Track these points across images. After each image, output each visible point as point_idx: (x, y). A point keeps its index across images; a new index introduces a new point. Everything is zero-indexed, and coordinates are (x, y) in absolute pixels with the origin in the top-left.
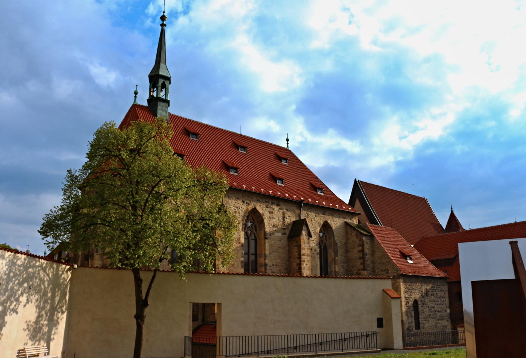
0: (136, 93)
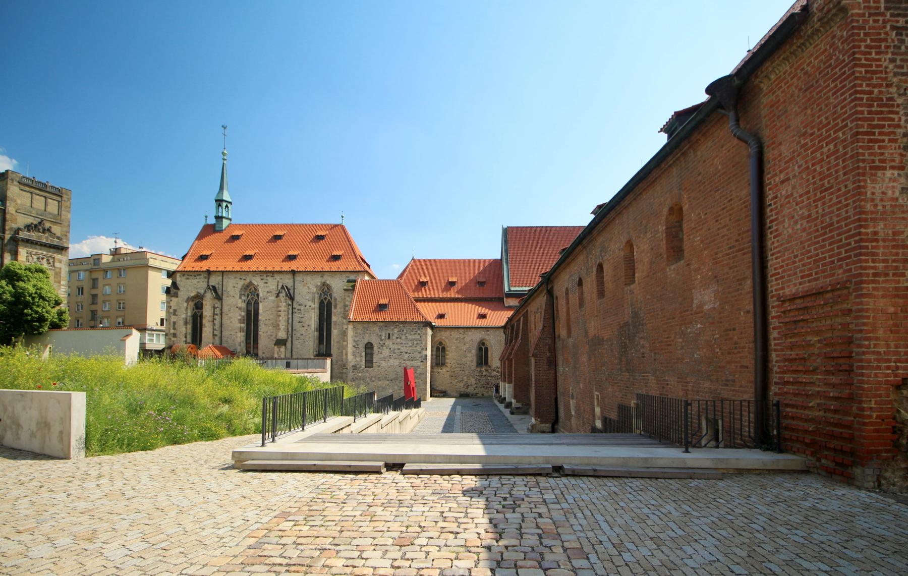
0: (206, 217)
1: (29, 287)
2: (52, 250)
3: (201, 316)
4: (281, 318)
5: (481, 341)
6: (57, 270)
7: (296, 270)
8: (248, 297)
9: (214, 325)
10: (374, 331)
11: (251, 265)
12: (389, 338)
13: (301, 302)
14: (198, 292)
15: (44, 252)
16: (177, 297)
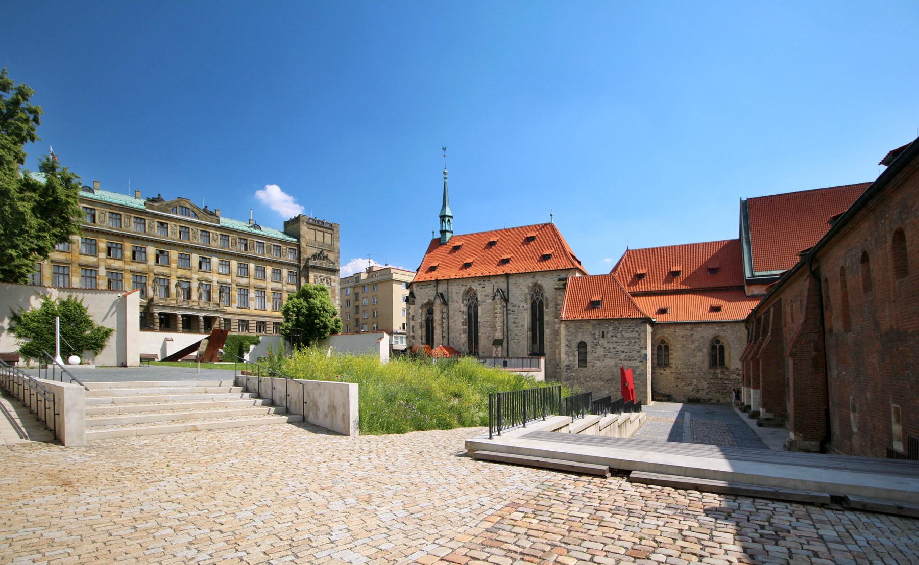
1: (316, 302)
2: (329, 273)
3: (432, 320)
4: (497, 319)
5: (715, 338)
6: (333, 288)
7: (509, 272)
8: (469, 301)
9: (443, 327)
10: (588, 329)
11: (470, 272)
12: (603, 336)
13: (514, 303)
15: (324, 275)
16: (414, 304)
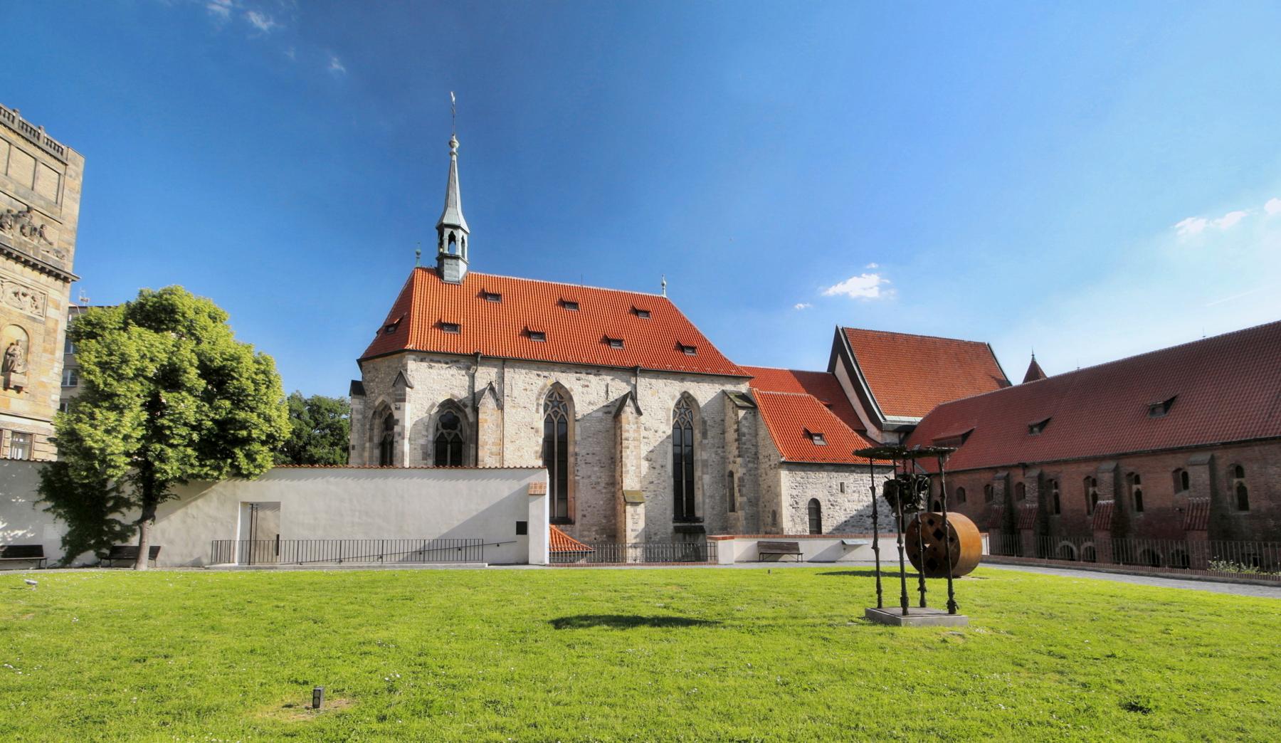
4: (628, 452)
12: (842, 491)
13: (647, 425)
14: (452, 395)
